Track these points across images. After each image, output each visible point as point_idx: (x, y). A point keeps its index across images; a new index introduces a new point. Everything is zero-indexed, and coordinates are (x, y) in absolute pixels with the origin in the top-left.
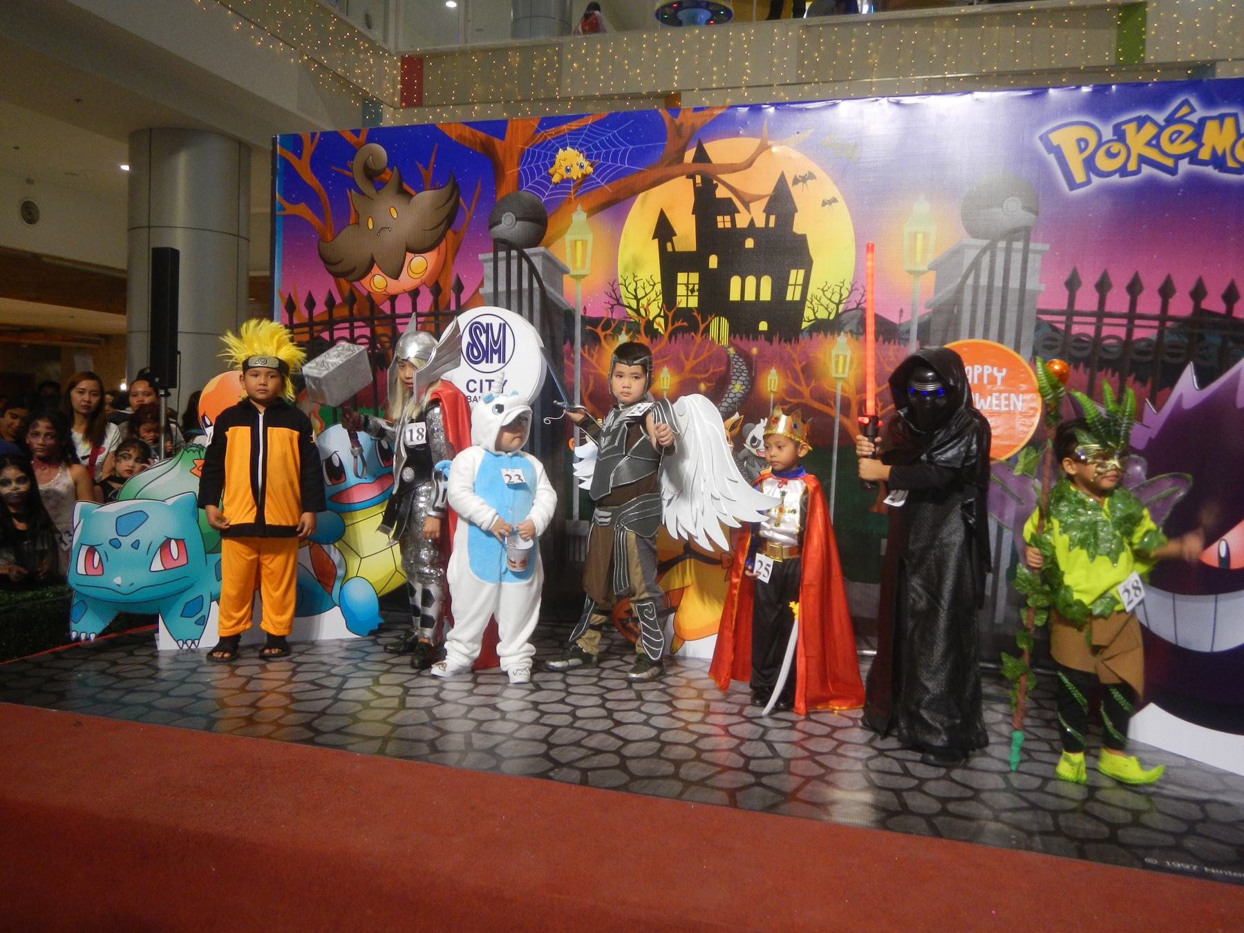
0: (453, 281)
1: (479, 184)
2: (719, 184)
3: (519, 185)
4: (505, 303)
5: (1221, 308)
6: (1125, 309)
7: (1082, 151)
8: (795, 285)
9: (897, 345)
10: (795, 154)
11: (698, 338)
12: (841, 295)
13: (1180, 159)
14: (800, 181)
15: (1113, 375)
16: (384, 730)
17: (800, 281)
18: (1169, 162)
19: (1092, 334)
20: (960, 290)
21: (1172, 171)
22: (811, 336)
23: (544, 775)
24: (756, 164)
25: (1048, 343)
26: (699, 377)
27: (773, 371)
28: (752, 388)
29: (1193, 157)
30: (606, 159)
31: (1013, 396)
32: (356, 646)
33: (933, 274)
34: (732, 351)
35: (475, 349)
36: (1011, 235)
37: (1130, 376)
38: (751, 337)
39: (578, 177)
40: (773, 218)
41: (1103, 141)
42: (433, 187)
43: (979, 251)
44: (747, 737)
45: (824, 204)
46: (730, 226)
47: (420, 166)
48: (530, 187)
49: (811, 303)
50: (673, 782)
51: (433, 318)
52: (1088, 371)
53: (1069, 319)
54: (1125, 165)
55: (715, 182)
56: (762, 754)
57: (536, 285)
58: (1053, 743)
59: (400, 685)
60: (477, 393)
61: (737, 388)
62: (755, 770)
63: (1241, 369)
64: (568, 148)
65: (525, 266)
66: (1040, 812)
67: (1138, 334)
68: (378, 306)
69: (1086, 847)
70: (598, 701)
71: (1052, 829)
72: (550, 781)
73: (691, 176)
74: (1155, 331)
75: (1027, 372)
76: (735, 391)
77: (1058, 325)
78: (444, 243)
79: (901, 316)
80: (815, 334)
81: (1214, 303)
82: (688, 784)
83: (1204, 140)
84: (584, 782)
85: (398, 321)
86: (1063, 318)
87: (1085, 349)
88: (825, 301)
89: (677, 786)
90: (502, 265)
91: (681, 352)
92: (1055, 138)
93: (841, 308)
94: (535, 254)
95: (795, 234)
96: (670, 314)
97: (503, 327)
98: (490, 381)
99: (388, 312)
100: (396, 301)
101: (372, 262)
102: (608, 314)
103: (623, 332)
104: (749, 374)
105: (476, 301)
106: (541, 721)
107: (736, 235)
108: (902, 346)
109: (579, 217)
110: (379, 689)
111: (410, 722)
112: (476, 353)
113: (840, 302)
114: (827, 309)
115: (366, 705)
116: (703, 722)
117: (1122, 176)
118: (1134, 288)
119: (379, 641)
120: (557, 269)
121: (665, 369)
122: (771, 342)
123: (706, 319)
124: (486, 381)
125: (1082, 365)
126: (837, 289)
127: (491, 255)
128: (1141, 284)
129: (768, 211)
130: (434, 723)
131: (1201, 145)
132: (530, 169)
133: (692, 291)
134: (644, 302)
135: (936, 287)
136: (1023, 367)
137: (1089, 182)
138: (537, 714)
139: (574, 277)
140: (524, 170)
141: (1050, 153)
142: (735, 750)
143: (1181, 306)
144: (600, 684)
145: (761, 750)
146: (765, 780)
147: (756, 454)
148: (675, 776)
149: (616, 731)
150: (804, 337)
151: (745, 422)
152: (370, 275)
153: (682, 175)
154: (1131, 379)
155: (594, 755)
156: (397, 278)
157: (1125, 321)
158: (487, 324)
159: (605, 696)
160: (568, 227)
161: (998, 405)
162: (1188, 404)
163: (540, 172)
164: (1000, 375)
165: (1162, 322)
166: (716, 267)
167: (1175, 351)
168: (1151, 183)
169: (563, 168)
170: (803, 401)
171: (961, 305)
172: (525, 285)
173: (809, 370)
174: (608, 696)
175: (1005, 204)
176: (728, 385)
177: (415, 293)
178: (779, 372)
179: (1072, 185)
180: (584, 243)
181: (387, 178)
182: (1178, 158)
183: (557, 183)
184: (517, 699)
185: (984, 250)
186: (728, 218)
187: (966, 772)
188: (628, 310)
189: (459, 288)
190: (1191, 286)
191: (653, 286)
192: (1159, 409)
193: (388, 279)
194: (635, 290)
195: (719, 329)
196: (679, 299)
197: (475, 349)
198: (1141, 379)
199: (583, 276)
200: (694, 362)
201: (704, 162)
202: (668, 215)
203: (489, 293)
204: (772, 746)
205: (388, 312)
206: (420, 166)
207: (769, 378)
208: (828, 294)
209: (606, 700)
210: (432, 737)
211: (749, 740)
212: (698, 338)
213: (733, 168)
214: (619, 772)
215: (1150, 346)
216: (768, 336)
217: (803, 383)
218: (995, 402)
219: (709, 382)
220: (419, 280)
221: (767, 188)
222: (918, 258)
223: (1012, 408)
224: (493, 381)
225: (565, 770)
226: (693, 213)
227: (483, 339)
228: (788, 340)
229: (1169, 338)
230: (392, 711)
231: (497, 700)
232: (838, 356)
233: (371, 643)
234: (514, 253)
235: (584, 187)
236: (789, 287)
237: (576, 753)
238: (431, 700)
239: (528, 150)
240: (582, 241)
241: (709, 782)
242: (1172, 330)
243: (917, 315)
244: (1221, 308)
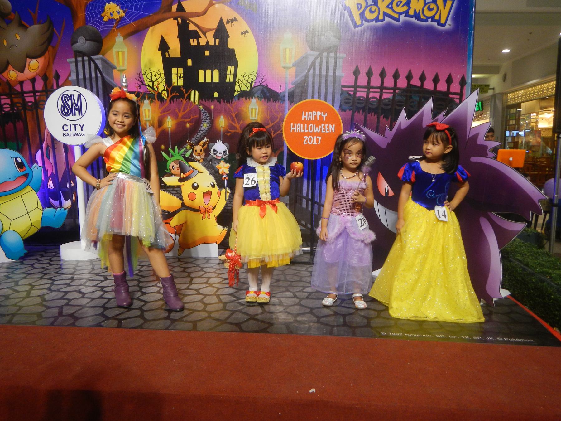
0: (54, 74)
1: (64, 21)
2: (190, 23)
3: (86, 21)
4: (83, 85)
5: (418, 84)
6: (379, 85)
7: (359, 9)
8: (230, 74)
9: (279, 104)
10: (227, 8)
11: (184, 101)
12: (252, 79)
14: (230, 22)
15: (374, 115)
16: (13, 310)
17: (233, 72)
18: (396, 16)
19: (365, 97)
20: (307, 76)
22: (239, 100)
23: (99, 325)
24: (207, 13)
25: (347, 101)
26: (186, 120)
27: (222, 117)
28: (212, 125)
29: (406, 14)
30: (131, 9)
31: (330, 126)
32: (12, 266)
33: (295, 68)
34: (201, 107)
35: (65, 108)
36: (329, 50)
37: (382, 115)
38: (210, 100)
39: (117, 18)
40: (218, 40)
41: (368, 5)
42: (38, 23)
43: (315, 57)
44: (208, 294)
45: (242, 33)
46: (197, 44)
47: (31, 12)
48: (92, 23)
49: (238, 83)
50: (166, 321)
51: (44, 93)
52: (364, 113)
53: (355, 89)
54: (378, 17)
55: (188, 22)
56: (214, 302)
57: (99, 75)
59: (30, 284)
60: (69, 132)
61: (205, 126)
62: (209, 310)
63: (424, 110)
64: (111, 3)
65: (92, 65)
66: (338, 316)
67: (385, 96)
68: (13, 87)
69: (358, 331)
70: (136, 283)
71: (343, 323)
72: (101, 328)
73: (176, 18)
74: (392, 94)
75: (336, 113)
76: (204, 127)
77: (350, 92)
78: (47, 51)
79: (280, 89)
80: (241, 98)
81: (416, 82)
82: (174, 321)
84: (119, 326)
85: (25, 95)
86: (353, 89)
87: (362, 103)
88: (245, 82)
89: (168, 322)
90: (80, 65)
91: (176, 108)
92: (347, 3)
93: (253, 85)
94: (98, 59)
95: (229, 48)
96: (170, 89)
97: (80, 96)
98: (75, 125)
99: (19, 90)
100: (24, 85)
101: (8, 64)
102: (137, 90)
103: (146, 99)
104: (210, 119)
105: (67, 82)
106: (103, 296)
107: (200, 49)
108: (282, 103)
109: (119, 39)
110: (17, 288)
111: (30, 304)
112: (66, 111)
113: (252, 82)
114: (246, 86)
115: (7, 297)
116: (188, 288)
117: (376, 22)
118: (383, 75)
119: (25, 262)
120: (110, 67)
121: (169, 117)
122: (220, 103)
123: (188, 91)
124: (73, 125)
125: (361, 111)
126: (250, 76)
127: (74, 59)
129: (215, 37)
130: (44, 303)
131: (410, 8)
132: (92, 14)
133: (180, 77)
134: (156, 83)
135: (296, 75)
136: (334, 110)
137: (362, 24)
138: (102, 293)
139: (119, 70)
140: (88, 14)
142: (201, 301)
143: (402, 83)
144: (139, 274)
145: (214, 299)
146: (213, 315)
147: (216, 157)
148: (168, 318)
149: (141, 298)
150: (236, 100)
151: (210, 142)
152: (7, 71)
153: (171, 18)
154: (382, 117)
155: (127, 311)
156: (22, 70)
157: (379, 90)
158: (71, 95)
159: (140, 280)
160: (114, 44)
161: (324, 130)
162: (403, 127)
163: (97, 16)
164: (324, 116)
165: (395, 91)
166: (191, 65)
167: (400, 103)
168: (389, 25)
169: (109, 13)
170: (237, 131)
171: (307, 83)
172: (93, 75)
173: (239, 116)
174: (141, 280)
175: (326, 34)
176: (200, 124)
177: (33, 80)
178: (224, 118)
179: (355, 26)
180: (123, 53)
181: (12, 17)
182: (400, 14)
183: (106, 22)
184: (93, 286)
185: (317, 57)
186: (195, 40)
187: (308, 300)
188: (148, 87)
189: (57, 77)
190: (406, 73)
191: (160, 75)
192: (391, 130)
193: (17, 72)
194: (151, 77)
195: (195, 96)
196: (173, 81)
197: (65, 108)
198: (386, 117)
199: (123, 70)
200: (183, 114)
201: (182, 11)
202: (165, 38)
203: (74, 80)
204: (219, 297)
205: (19, 90)
206: (31, 12)
207: (220, 120)
208: (246, 78)
209: (140, 282)
210: (41, 310)
211: (208, 295)
212: (184, 101)
213: (197, 15)
214: (138, 319)
215: (389, 101)
216: (219, 99)
217: (236, 122)
218: (323, 129)
219: (191, 123)
220: (35, 73)
221: (215, 25)
222: (287, 61)
223: (330, 131)
224: (77, 125)
225: (110, 321)
226: (178, 38)
227: (69, 103)
228: (228, 101)
229: (397, 98)
230: (21, 299)
231: (81, 287)
232: (252, 109)
233: (19, 264)
234: (86, 58)
235: (121, 24)
236: (227, 75)
237: (118, 311)
238: (45, 291)
239: (89, 3)
240: (122, 51)
241: (184, 319)
242: (399, 95)
243: (288, 88)
244: (418, 84)
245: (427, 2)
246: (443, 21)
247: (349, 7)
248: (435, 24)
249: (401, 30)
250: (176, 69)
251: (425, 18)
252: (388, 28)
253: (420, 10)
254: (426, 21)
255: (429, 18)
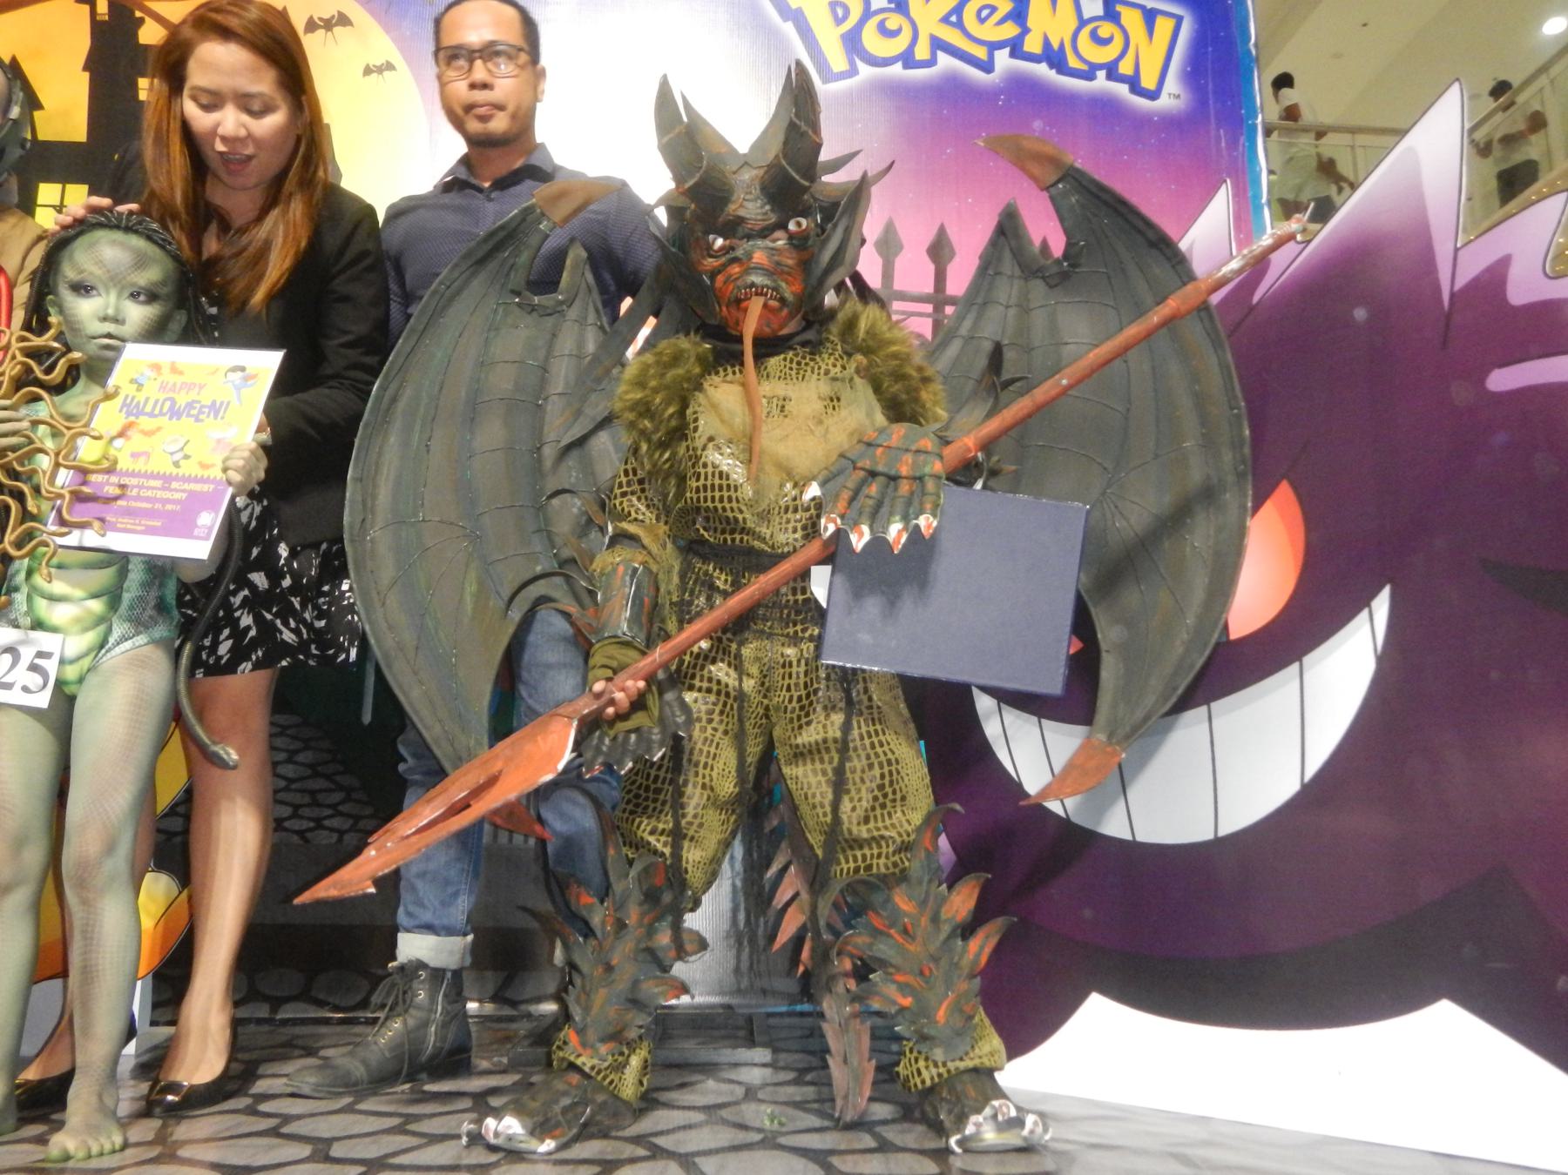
2: (148, 21)
6: (929, 289)
7: (839, 21)
13: (1000, 48)
14: (320, 27)
18: (981, 53)
21: (987, 67)
41: (874, 7)
45: (368, 71)
55: (138, 14)
58: (878, 1129)
83: (1030, 24)
117: (906, 66)
128: (949, 243)
131: (1026, 31)
137: (853, 71)
141: (785, 21)
157: (929, 308)
182: (993, 46)
245: (1086, 16)
246: (1148, 82)
247: (799, 11)
248: (1122, 90)
249: (999, 100)
250: (59, 187)
251: (1084, 67)
252: (952, 92)
253: (1062, 45)
254: (1089, 75)
255: (1101, 67)
